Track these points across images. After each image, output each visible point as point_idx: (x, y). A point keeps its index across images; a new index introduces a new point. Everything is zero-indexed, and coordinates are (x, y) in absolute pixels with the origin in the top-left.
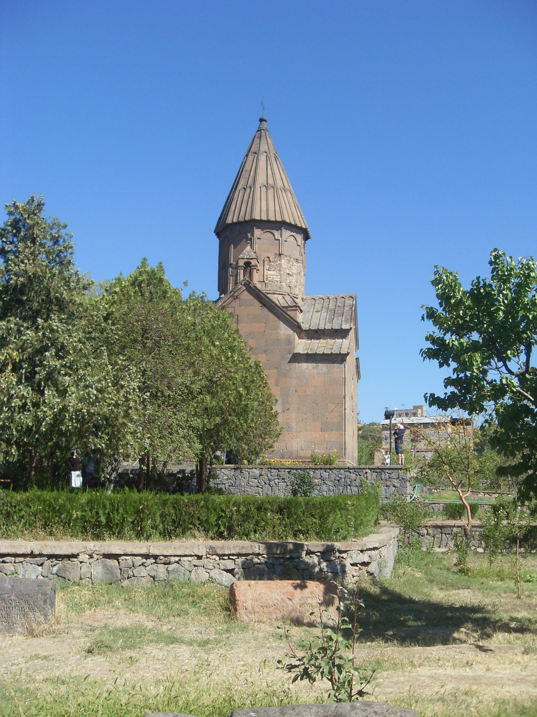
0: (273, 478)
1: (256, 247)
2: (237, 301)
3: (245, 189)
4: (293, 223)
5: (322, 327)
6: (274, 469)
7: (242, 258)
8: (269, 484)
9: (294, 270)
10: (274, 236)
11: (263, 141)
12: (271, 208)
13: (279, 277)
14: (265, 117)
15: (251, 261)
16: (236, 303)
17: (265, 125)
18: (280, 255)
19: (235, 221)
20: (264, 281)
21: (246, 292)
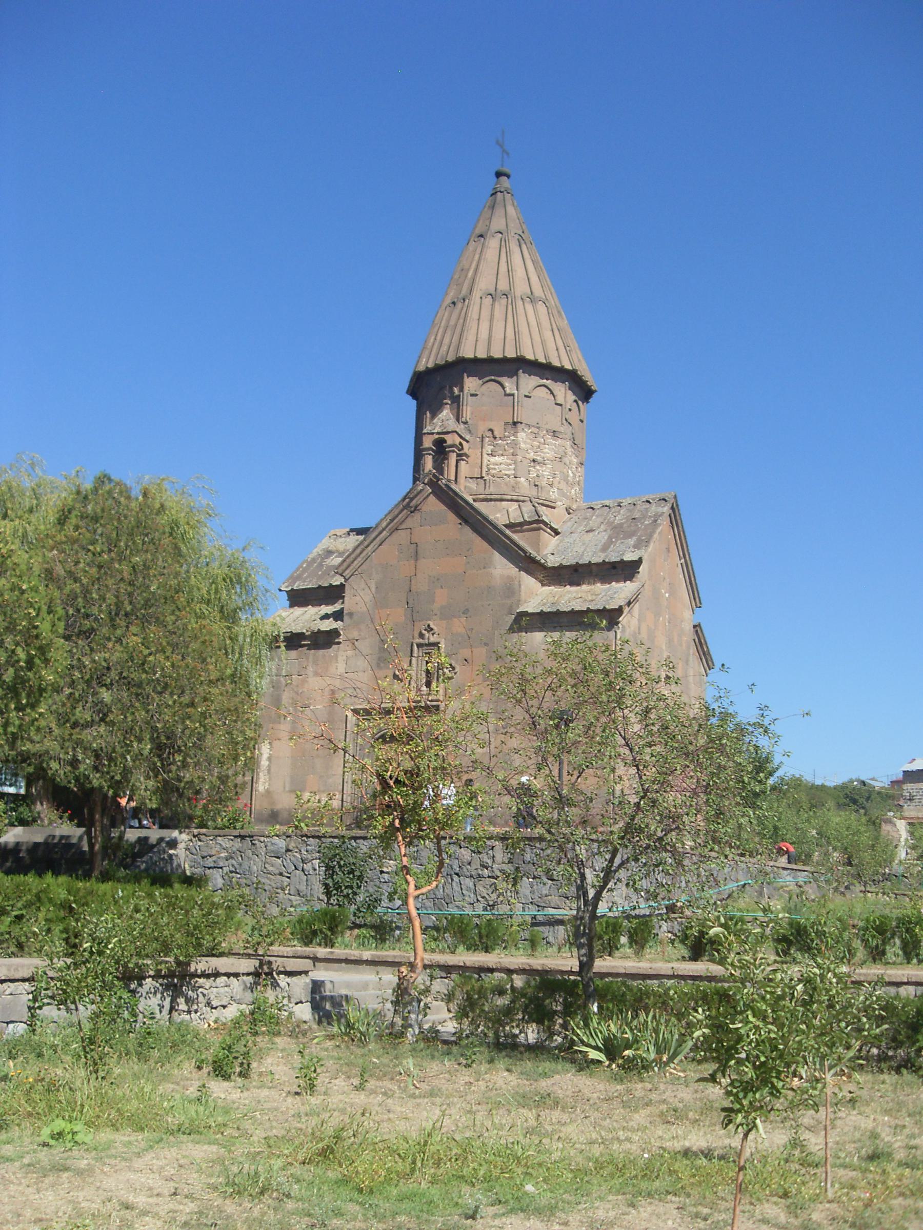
0: (309, 856)
1: (467, 412)
2: (417, 515)
3: (454, 303)
4: (542, 360)
5: (585, 560)
6: (313, 837)
7: (428, 434)
8: (303, 870)
9: (548, 452)
10: (503, 387)
11: (499, 211)
12: (498, 335)
13: (513, 467)
14: (506, 169)
15: (446, 437)
16: (414, 521)
17: (505, 182)
18: (515, 424)
19: (430, 365)
20: (482, 478)
21: (432, 498)
